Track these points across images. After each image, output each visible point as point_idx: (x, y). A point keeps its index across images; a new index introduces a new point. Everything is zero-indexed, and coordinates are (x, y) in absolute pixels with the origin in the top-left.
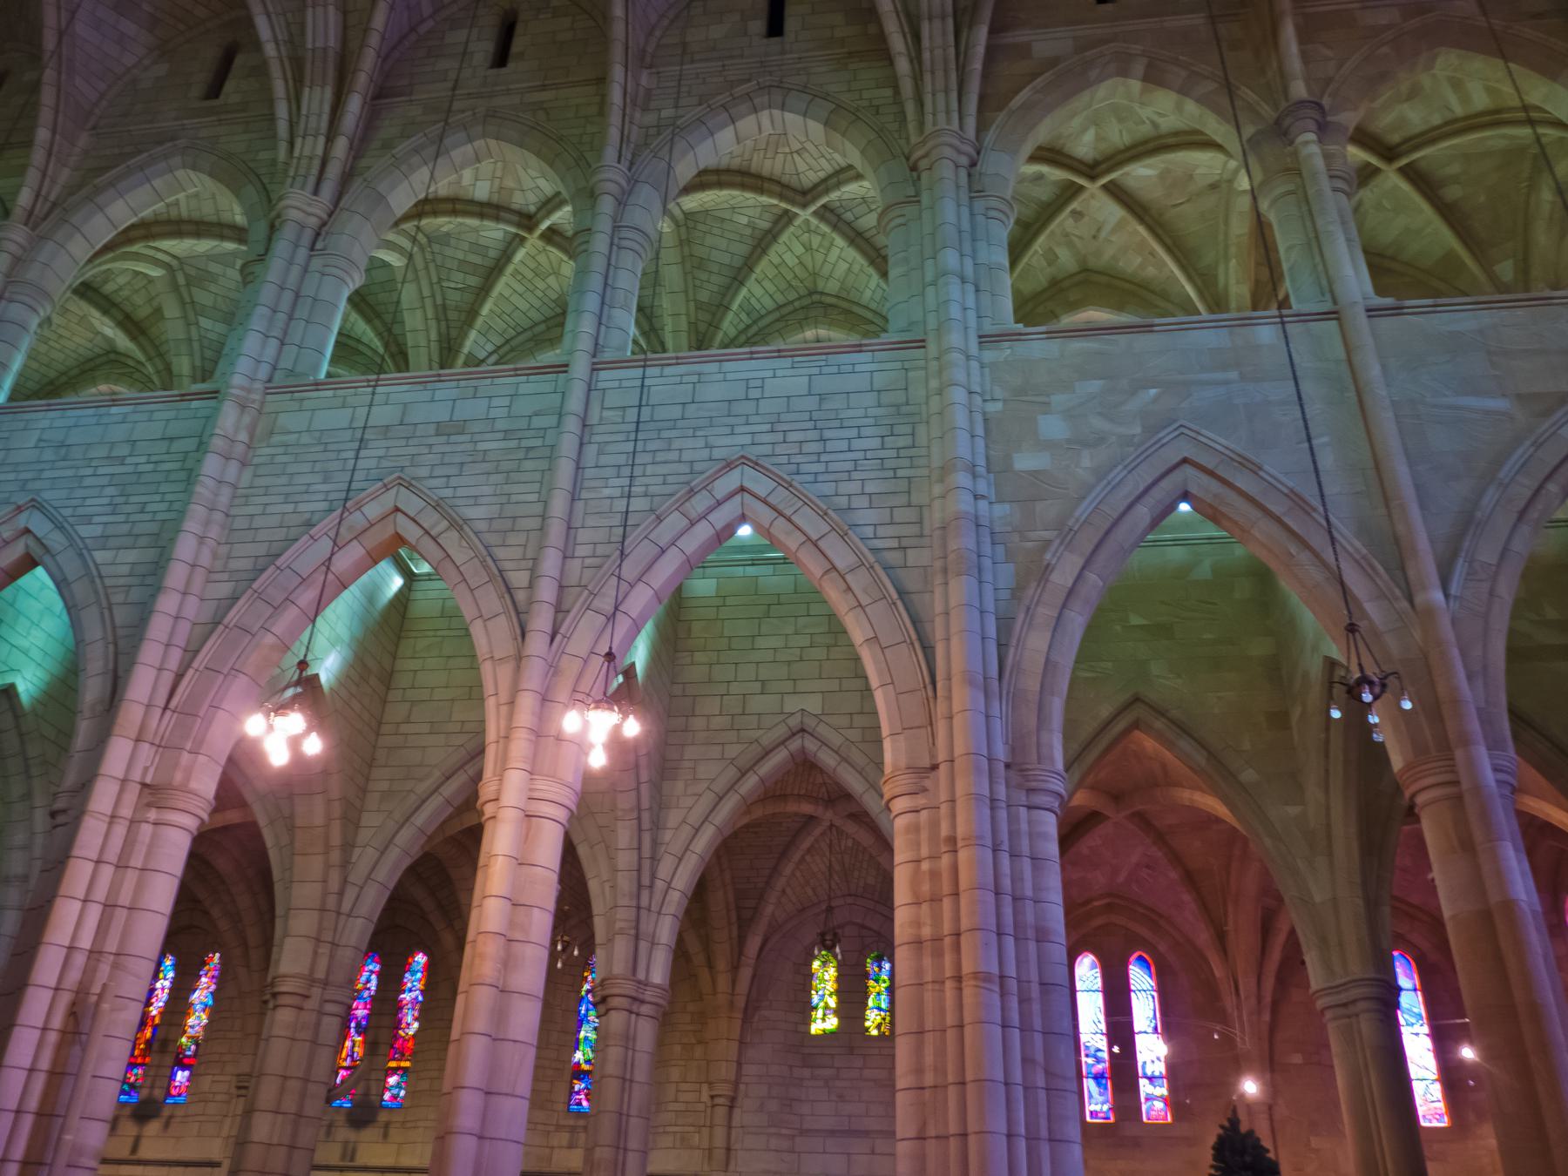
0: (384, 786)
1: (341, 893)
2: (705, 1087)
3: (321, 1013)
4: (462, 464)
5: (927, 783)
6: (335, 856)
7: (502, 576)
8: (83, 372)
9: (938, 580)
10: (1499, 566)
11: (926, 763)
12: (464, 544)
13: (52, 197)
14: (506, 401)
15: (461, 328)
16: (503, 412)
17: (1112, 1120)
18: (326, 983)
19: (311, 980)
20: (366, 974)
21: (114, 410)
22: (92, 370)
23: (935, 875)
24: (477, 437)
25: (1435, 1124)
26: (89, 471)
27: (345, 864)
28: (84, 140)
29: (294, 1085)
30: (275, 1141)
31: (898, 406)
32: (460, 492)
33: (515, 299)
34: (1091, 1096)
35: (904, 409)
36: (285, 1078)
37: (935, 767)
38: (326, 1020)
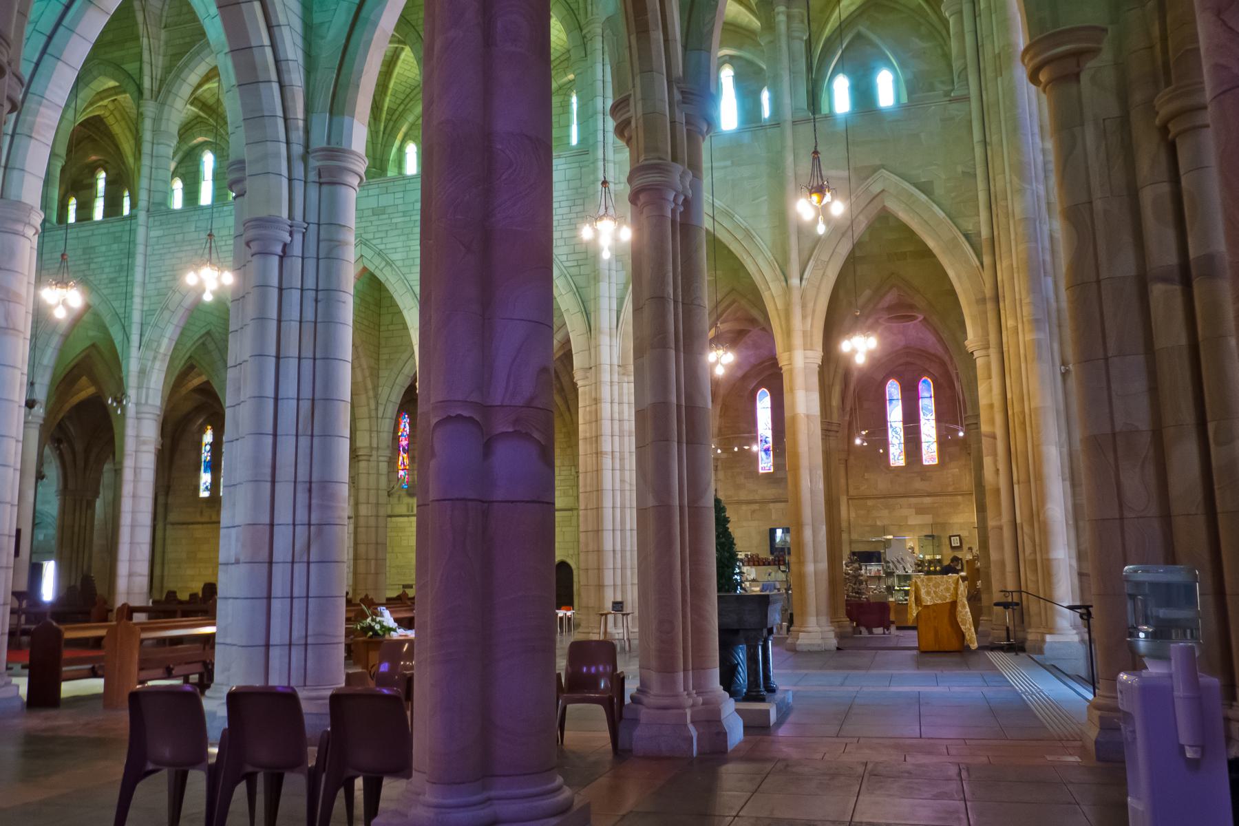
0: (386, 357)
1: (377, 409)
2: (573, 467)
3: (378, 462)
4: (387, 231)
5: (588, 375)
6: (371, 393)
7: (412, 288)
8: (187, 130)
9: (592, 282)
10: (828, 262)
11: (587, 366)
12: (393, 272)
13: (159, 77)
14: (401, 195)
15: (381, 95)
16: (401, 201)
17: (772, 471)
18: (378, 448)
19: (371, 448)
20: (403, 424)
21: (225, 208)
22: (190, 128)
23: (590, 412)
24: (391, 216)
25: (931, 463)
26: (223, 243)
27: (376, 396)
28: (163, 35)
29: (372, 492)
30: (370, 515)
31: (577, 189)
32: (389, 246)
33: (407, 73)
34: (762, 460)
35: (580, 190)
36: (368, 489)
37: (591, 368)
38: (381, 464)
